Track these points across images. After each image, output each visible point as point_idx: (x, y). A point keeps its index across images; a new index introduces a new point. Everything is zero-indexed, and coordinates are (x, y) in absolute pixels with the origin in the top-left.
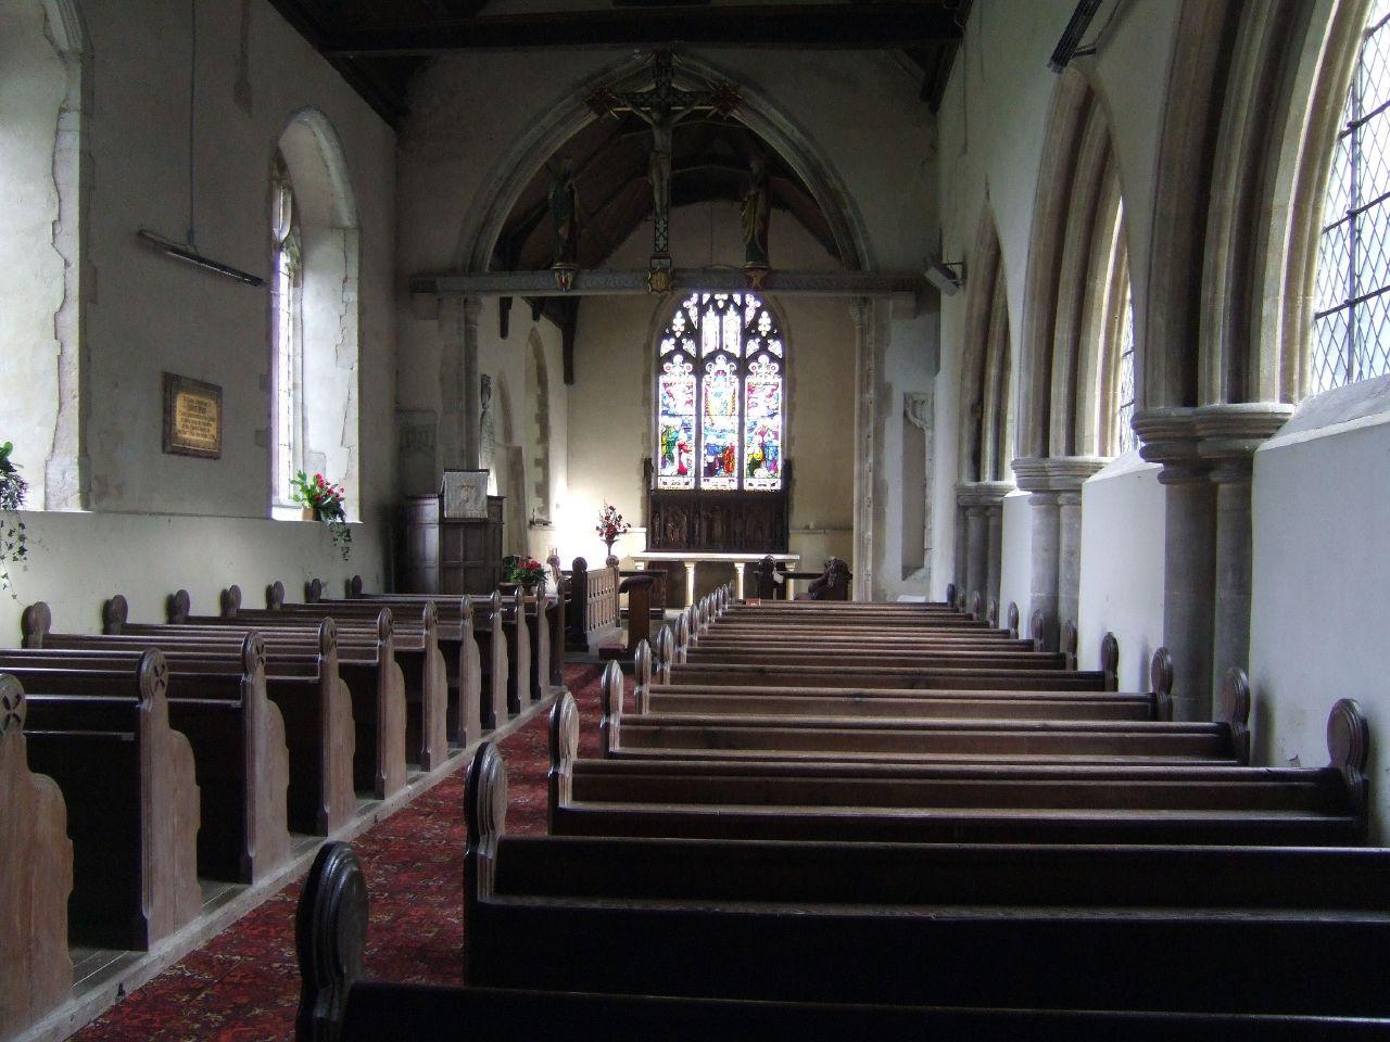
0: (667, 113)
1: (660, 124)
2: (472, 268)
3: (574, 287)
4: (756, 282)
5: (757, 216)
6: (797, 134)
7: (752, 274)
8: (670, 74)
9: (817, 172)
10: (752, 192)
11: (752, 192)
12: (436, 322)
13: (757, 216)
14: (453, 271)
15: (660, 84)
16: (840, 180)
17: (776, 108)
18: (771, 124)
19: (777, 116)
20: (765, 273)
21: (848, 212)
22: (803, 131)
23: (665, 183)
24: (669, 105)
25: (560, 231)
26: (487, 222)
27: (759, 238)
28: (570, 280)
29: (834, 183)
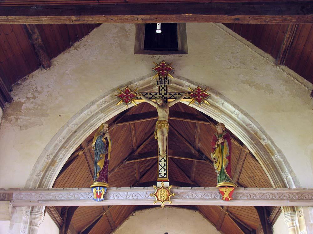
0: (165, 102)
1: (162, 106)
2: (41, 186)
3: (105, 198)
4: (226, 195)
5: (225, 157)
6: (241, 116)
7: (223, 190)
8: (167, 83)
9: (255, 138)
10: (220, 141)
11: (220, 141)
12: (9, 222)
13: (225, 157)
14: (26, 189)
15: (161, 88)
16: (269, 139)
17: (227, 102)
18: (222, 111)
19: (228, 107)
20: (232, 189)
21: (276, 157)
22: (243, 112)
23: (165, 138)
24: (167, 99)
25: (98, 164)
26: (53, 163)
27: (226, 169)
28: (103, 193)
29: (265, 141)
